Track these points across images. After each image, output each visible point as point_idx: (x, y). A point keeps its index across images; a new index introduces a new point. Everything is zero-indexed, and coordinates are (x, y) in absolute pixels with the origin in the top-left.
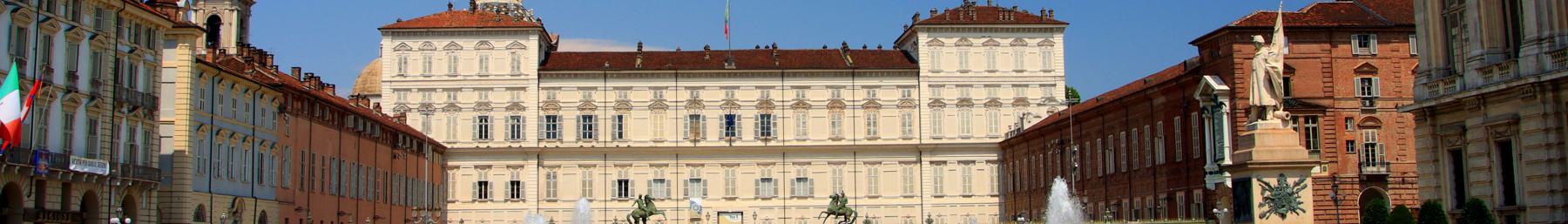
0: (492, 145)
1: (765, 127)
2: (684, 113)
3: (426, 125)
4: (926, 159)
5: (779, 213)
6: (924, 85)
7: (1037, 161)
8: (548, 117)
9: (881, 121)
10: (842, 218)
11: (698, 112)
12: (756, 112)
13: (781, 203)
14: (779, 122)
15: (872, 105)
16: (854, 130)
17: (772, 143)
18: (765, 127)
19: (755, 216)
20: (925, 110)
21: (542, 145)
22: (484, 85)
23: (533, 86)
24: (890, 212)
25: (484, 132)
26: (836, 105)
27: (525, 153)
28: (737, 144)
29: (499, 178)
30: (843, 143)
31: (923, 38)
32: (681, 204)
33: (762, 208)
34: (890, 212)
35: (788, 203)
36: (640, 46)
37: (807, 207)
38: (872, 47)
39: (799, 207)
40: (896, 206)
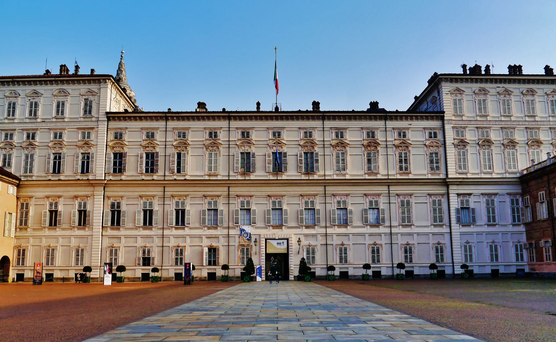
0: (62, 178)
1: (310, 163)
2: (237, 152)
4: (454, 190)
5: (321, 240)
6: (447, 127)
8: (115, 155)
9: (412, 159)
11: (246, 149)
12: (300, 151)
13: (323, 231)
14: (320, 159)
15: (404, 145)
16: (387, 167)
17: (316, 177)
18: (310, 163)
19: (299, 241)
20: (452, 152)
21: (107, 178)
22: (59, 125)
23: (103, 127)
24: (423, 239)
25: (57, 169)
26: (371, 144)
27: (92, 184)
28: (284, 177)
29: (68, 210)
30: (379, 177)
31: (446, 88)
32: (232, 232)
33: (306, 235)
34: (423, 239)
35: (329, 231)
37: (346, 235)
39: (338, 235)
40: (427, 234)
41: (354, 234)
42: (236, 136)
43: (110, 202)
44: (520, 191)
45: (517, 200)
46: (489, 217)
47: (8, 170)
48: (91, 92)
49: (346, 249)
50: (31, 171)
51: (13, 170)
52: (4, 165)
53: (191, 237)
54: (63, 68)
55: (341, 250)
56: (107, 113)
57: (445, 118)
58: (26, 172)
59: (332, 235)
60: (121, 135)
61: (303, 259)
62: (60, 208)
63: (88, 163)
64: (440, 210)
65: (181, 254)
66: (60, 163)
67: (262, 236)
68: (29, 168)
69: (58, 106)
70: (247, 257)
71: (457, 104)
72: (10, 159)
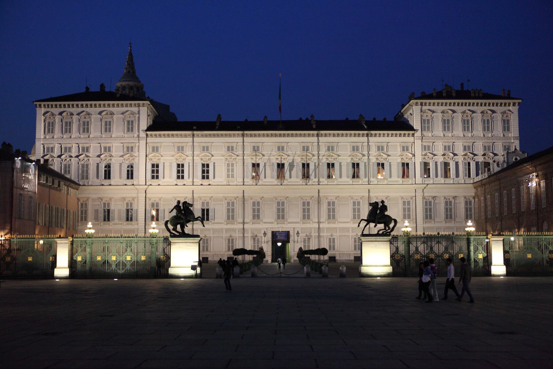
2: (249, 162)
3: (68, 168)
7: (509, 195)
10: (381, 226)
23: (143, 143)
36: (219, 116)
37: (336, 228)
38: (380, 118)
39: (328, 229)
41: (340, 228)
42: (249, 151)
43: (150, 202)
44: (473, 194)
45: (470, 202)
46: (447, 215)
47: (68, 176)
48: (133, 113)
49: (334, 239)
50: (87, 178)
51: (73, 178)
52: (65, 172)
53: (215, 231)
54: (102, 86)
55: (330, 239)
56: (147, 130)
57: (415, 135)
58: (83, 178)
59: (323, 228)
60: (157, 148)
61: (301, 248)
62: (112, 208)
63: (132, 171)
64: (409, 209)
65: (207, 243)
66: (109, 171)
67: (269, 229)
68: (84, 174)
69: (106, 125)
70: (258, 246)
71: (426, 124)
72: (69, 167)
